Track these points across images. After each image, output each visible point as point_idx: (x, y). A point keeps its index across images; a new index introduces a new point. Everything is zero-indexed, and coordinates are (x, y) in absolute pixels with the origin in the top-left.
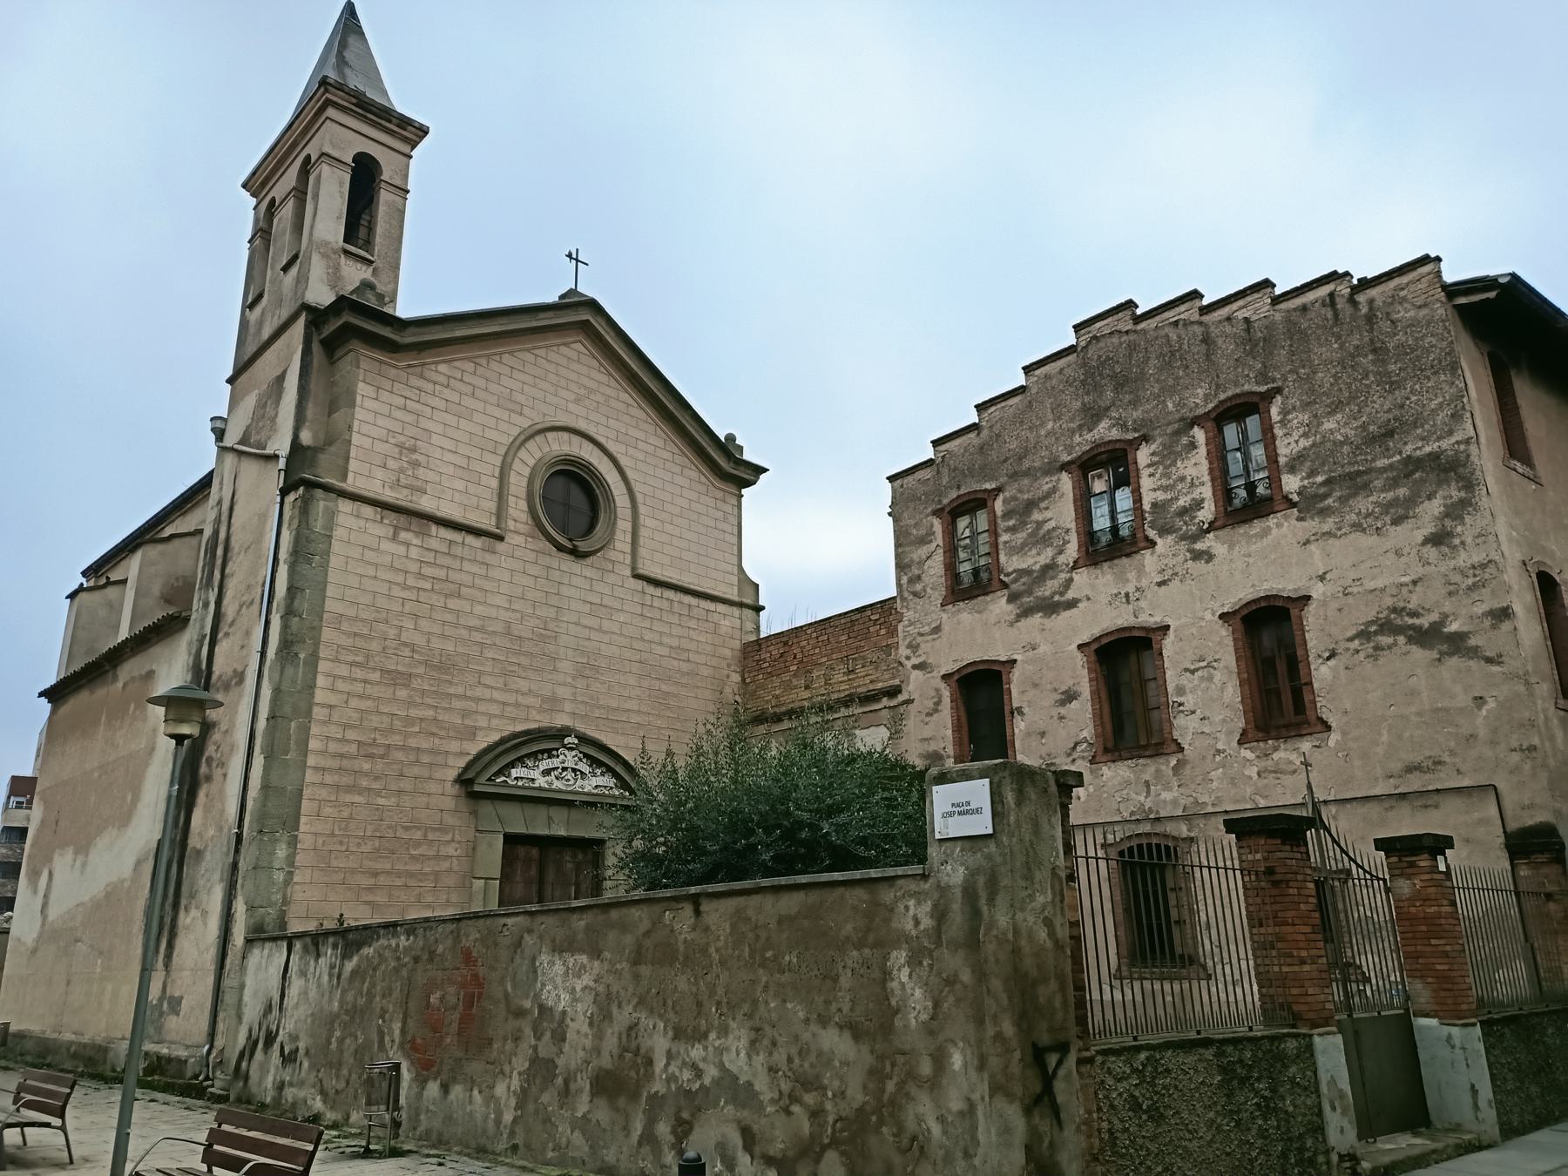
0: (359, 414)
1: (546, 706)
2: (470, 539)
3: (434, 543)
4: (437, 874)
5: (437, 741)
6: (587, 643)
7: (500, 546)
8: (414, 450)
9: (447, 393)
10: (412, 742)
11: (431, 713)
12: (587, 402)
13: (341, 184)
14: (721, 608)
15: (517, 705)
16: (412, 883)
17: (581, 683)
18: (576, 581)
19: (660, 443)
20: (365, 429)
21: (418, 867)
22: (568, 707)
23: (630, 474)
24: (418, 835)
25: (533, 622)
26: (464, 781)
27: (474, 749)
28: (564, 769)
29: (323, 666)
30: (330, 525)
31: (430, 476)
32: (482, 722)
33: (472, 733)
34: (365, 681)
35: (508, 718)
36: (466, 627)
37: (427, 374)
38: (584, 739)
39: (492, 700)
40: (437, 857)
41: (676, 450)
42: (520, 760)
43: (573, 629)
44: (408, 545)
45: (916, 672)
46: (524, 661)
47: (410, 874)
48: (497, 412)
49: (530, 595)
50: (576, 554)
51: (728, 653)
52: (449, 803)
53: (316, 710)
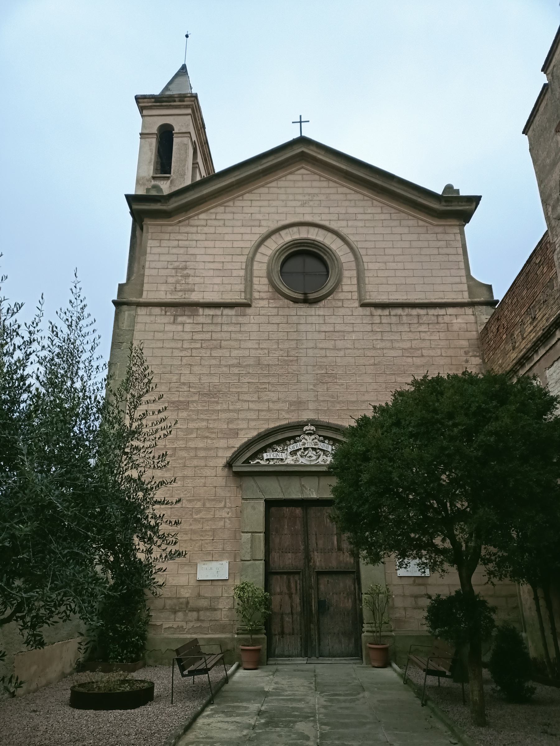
0: (149, 257)
1: (293, 408)
2: (227, 311)
3: (201, 319)
4: (214, 531)
5: (209, 441)
6: (324, 360)
7: (249, 311)
8: (186, 268)
9: (206, 230)
10: (192, 444)
11: (204, 424)
12: (311, 203)
13: (150, 145)
14: (450, 311)
15: (269, 410)
16: (195, 537)
17: (321, 389)
18: (314, 319)
19: (379, 210)
20: (153, 265)
21: (200, 526)
22: (311, 406)
23: (351, 239)
24: (199, 505)
25: (278, 353)
26: (229, 465)
27: (238, 443)
28: (306, 449)
30: (133, 323)
31: (197, 280)
32: (243, 425)
33: (235, 433)
35: (263, 420)
36: (226, 366)
37: (192, 222)
38: (320, 426)
39: (249, 409)
40: (214, 519)
41: (393, 211)
42: (270, 446)
43: (311, 352)
44: (183, 324)
46: (273, 380)
47: (193, 532)
48: (243, 230)
49: (274, 336)
50: (306, 301)
51: (465, 343)
52: (221, 481)
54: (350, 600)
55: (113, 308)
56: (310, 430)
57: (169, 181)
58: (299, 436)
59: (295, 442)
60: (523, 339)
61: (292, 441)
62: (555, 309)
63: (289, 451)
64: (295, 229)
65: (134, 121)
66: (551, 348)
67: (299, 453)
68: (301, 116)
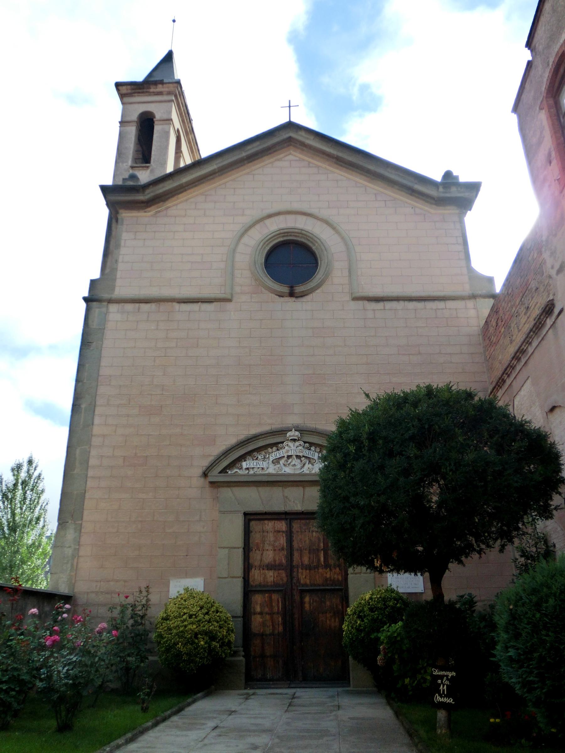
0: (123, 251)
2: (205, 306)
7: (229, 306)
26: (205, 475)
28: (289, 457)
29: (98, 410)
34: (128, 416)
37: (171, 212)
38: (302, 431)
45: (561, 275)
50: (292, 294)
53: (94, 439)
54: (337, 620)
55: (84, 305)
56: (293, 436)
57: (149, 171)
58: (283, 443)
59: (278, 450)
60: (519, 331)
61: (275, 448)
62: (545, 297)
63: (271, 459)
64: (281, 217)
65: (113, 108)
66: (543, 339)
67: (282, 462)
68: (290, 101)
